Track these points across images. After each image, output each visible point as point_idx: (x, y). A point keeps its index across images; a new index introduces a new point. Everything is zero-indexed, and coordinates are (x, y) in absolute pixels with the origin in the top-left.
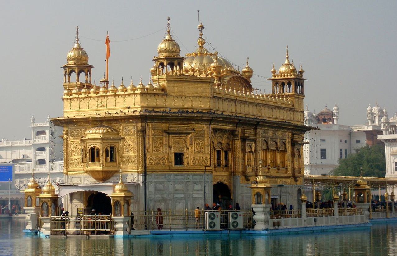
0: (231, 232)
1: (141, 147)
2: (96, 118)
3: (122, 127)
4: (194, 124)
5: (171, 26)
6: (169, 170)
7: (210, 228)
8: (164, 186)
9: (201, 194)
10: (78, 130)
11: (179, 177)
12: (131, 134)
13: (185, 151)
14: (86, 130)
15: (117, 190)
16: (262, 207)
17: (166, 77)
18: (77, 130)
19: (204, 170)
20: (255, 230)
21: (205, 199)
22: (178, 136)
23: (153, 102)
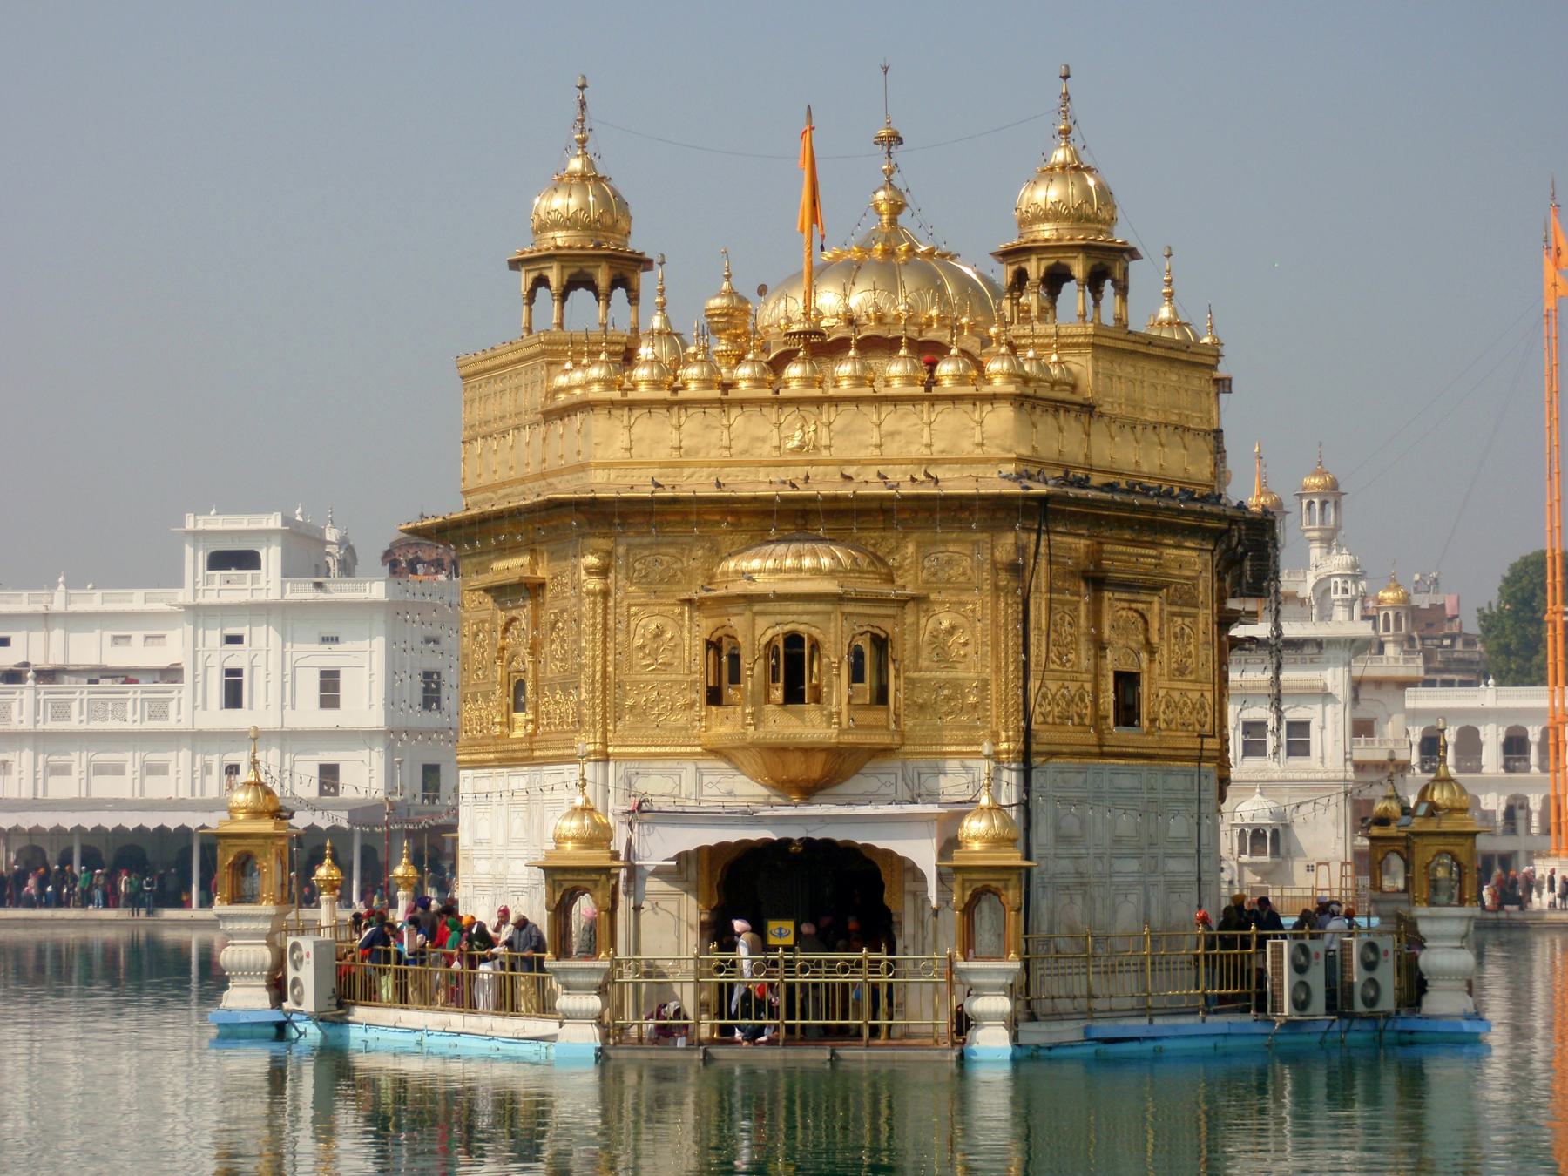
0: (1356, 1025)
1: (1013, 642)
2: (770, 500)
3: (911, 549)
4: (1169, 546)
5: (1076, 106)
6: (1097, 750)
7: (1294, 1011)
8: (1083, 822)
9: (1186, 857)
10: (672, 550)
11: (1125, 782)
12: (962, 579)
13: (1144, 665)
14: (717, 555)
15: (975, 838)
16: (1461, 918)
17: (1090, 330)
18: (663, 550)
19: (1197, 753)
20: (1427, 1018)
21: (1199, 879)
22: (1124, 596)
23: (1064, 441)
